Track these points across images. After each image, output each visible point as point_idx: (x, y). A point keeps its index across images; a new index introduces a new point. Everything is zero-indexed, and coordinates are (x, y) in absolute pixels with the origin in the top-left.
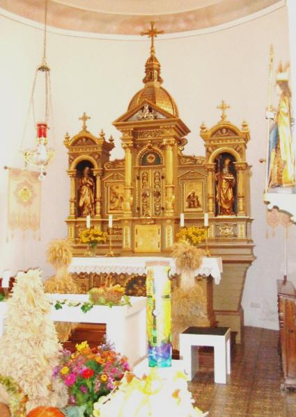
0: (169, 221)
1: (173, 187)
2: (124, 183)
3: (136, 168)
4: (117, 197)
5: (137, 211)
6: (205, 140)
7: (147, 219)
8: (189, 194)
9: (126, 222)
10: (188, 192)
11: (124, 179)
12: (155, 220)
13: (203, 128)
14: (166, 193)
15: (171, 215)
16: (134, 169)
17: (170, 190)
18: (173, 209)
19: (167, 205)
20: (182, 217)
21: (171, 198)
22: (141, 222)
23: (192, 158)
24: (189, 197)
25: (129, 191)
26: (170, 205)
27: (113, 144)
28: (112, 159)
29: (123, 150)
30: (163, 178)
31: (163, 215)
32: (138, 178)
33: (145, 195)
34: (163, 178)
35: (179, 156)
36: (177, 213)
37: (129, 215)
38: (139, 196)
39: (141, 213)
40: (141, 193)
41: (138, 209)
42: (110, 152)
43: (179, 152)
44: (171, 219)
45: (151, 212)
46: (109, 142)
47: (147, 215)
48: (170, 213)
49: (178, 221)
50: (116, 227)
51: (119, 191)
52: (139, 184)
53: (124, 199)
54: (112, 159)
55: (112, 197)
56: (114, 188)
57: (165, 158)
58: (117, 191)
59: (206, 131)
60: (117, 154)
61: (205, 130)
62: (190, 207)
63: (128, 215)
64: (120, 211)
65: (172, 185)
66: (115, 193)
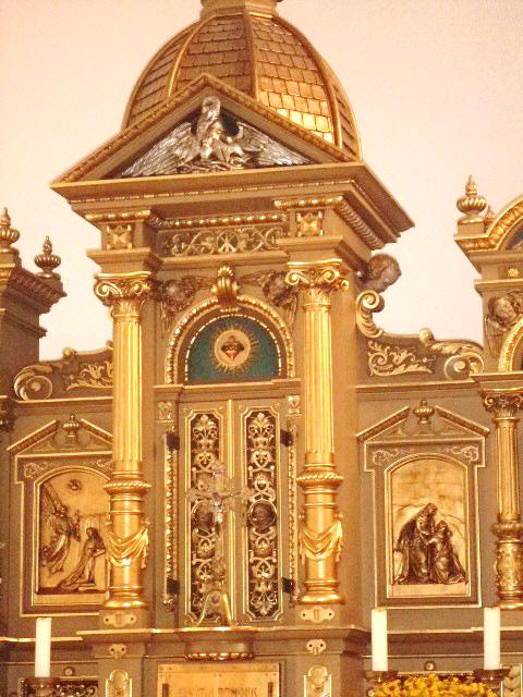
0: (316, 646)
1: (335, 484)
2: (106, 463)
3: (160, 395)
4: (73, 533)
5: (167, 599)
6: (478, 266)
7: (216, 639)
8: (410, 514)
9: (316, 646)
10: (403, 508)
11: (107, 441)
12: (249, 639)
13: (468, 209)
14: (304, 511)
15: (326, 614)
16: (153, 397)
17: (321, 497)
18: (335, 586)
19: (306, 568)
20: (379, 625)
21: (327, 535)
22: (187, 650)
23: (422, 350)
24: (410, 528)
25: (128, 504)
26: (321, 571)
27: (57, 278)
28: (50, 350)
29: (104, 311)
30: (287, 439)
31: (290, 619)
32: (174, 442)
33: (204, 523)
34: (287, 439)
35: (361, 339)
36: (353, 608)
37: (128, 619)
38: (176, 524)
39: (187, 606)
40: (189, 513)
41: (174, 587)
42: (44, 320)
43: (360, 319)
44: (327, 637)
45: (232, 600)
46: (36, 270)
47: (216, 616)
48: (320, 611)
49: (359, 642)
50: (68, 676)
51: (86, 503)
52: (177, 474)
53: (107, 540)
54: (50, 350)
55: (49, 532)
56: (60, 486)
57: (299, 351)
58: (75, 502)
59: (486, 223)
60: (75, 324)
61: (480, 217)
62: (412, 576)
63: (124, 617)
64: (92, 599)
65: (331, 475)
66: (63, 513)
